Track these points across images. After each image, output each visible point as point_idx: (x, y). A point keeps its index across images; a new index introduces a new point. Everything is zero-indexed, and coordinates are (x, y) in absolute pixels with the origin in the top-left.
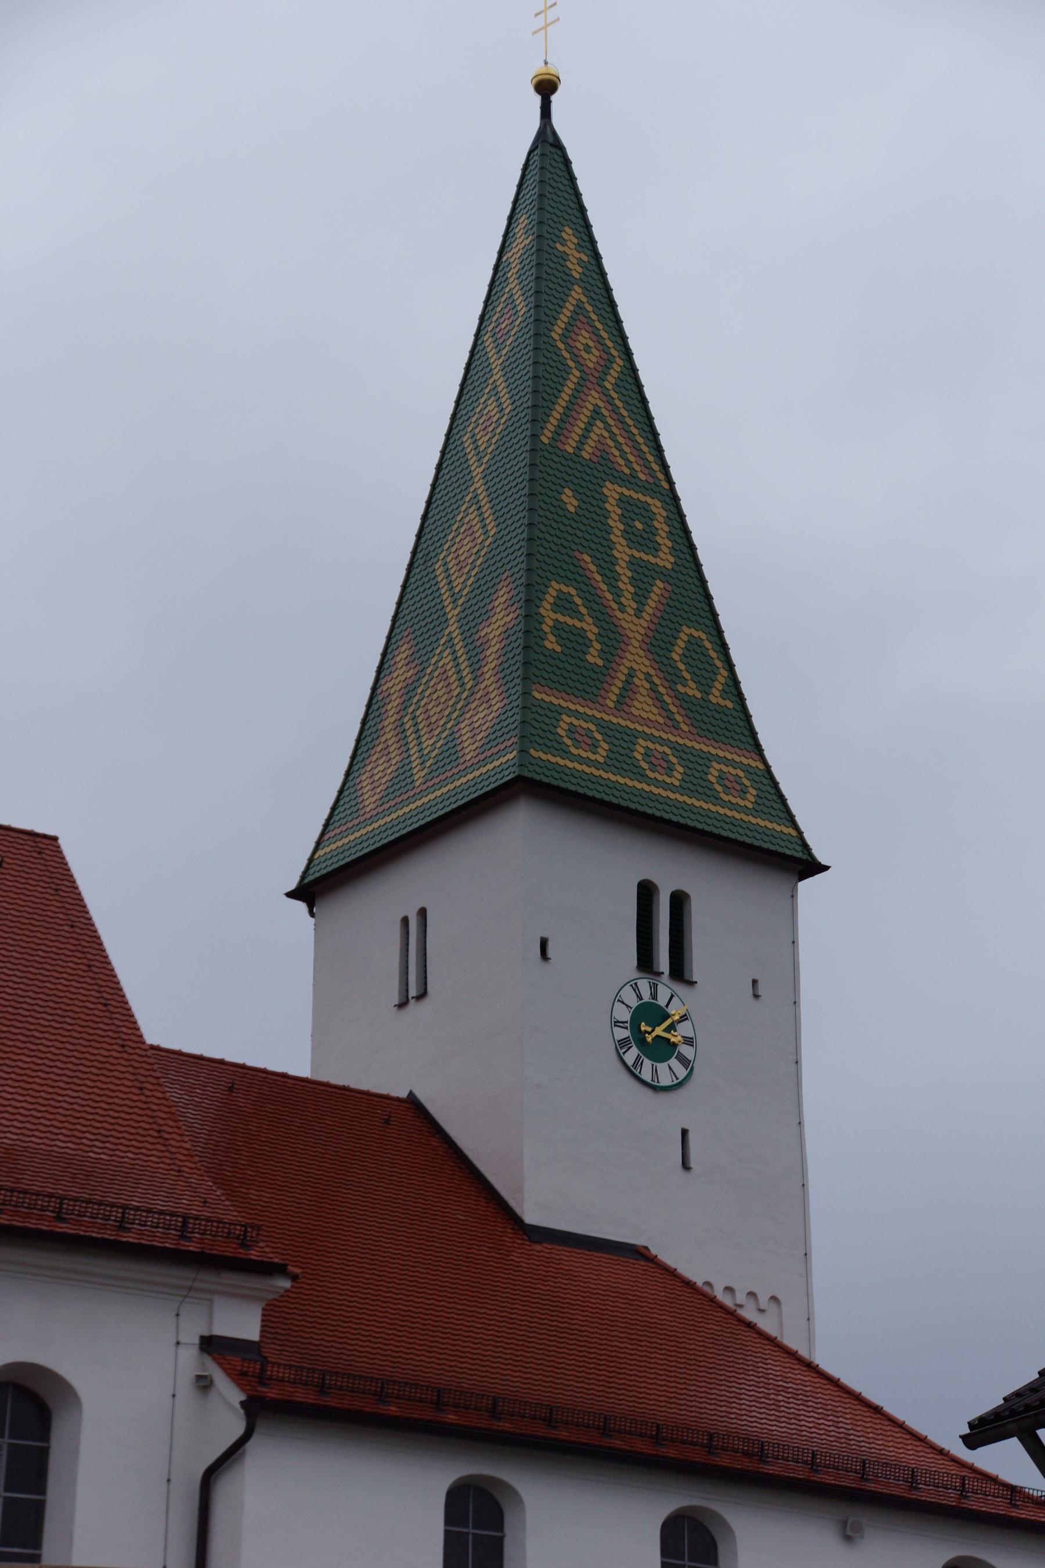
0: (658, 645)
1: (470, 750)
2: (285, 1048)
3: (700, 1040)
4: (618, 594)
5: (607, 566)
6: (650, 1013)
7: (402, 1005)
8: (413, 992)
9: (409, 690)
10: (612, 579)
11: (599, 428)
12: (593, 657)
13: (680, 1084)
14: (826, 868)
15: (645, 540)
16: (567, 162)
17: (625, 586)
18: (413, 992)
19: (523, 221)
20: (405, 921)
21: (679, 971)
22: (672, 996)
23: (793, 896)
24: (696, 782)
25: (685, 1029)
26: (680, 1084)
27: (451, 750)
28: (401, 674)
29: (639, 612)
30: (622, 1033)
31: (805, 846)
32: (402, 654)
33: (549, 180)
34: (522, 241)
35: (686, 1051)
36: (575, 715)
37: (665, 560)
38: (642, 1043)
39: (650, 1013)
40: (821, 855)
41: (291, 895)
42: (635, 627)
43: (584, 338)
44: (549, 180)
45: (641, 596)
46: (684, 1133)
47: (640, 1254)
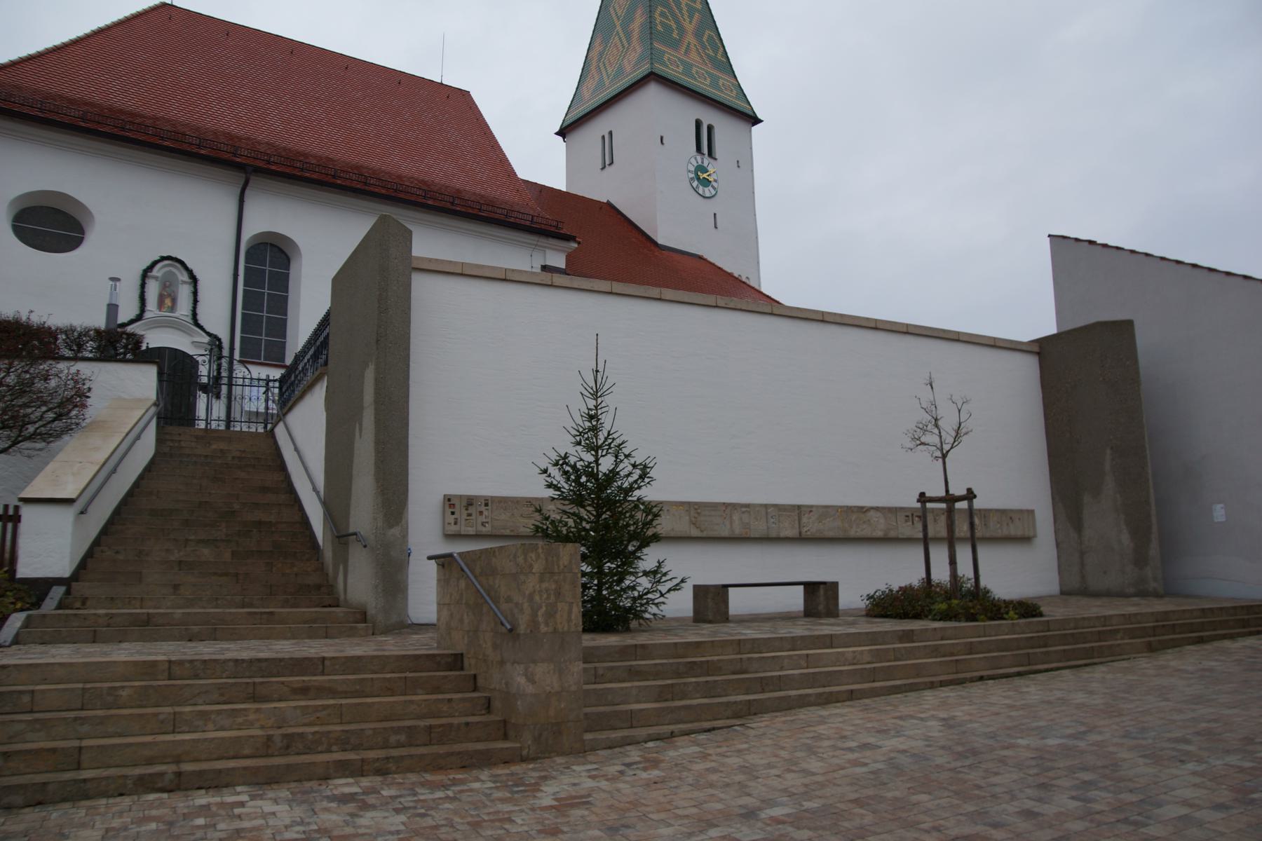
0: (698, 34)
1: (628, 68)
2: (558, 181)
6: (701, 169)
8: (607, 162)
9: (601, 54)
10: (681, 10)
17: (684, 11)
18: (608, 161)
21: (710, 154)
24: (715, 84)
27: (620, 71)
32: (598, 41)
35: (715, 184)
36: (669, 54)
38: (698, 179)
39: (701, 169)
40: (760, 116)
42: (690, 27)
45: (691, 17)
47: (700, 258)
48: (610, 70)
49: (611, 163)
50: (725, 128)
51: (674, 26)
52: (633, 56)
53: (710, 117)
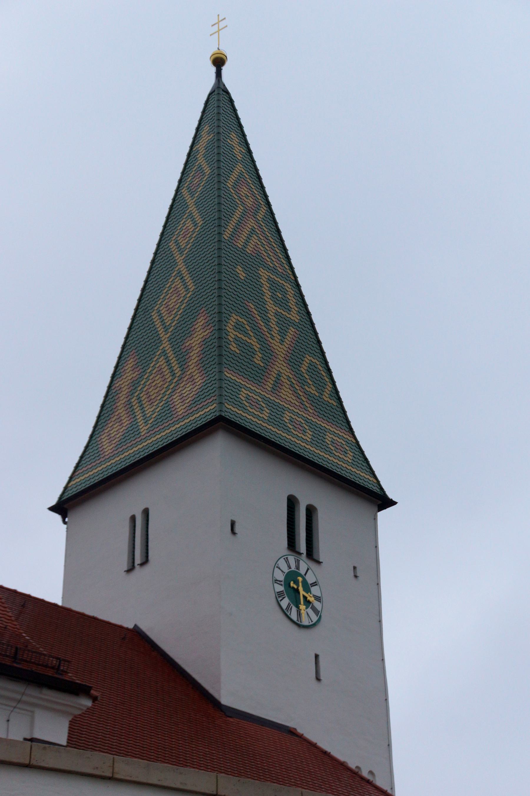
0: (294, 361)
1: (180, 409)
3: (324, 599)
4: (270, 329)
5: (263, 313)
7: (131, 569)
8: (138, 560)
9: (134, 384)
11: (254, 239)
12: (258, 360)
13: (314, 625)
14: (394, 503)
15: (283, 303)
16: (231, 101)
19: (206, 128)
20: (133, 519)
21: (311, 554)
22: (308, 569)
23: (375, 519)
25: (315, 590)
26: (314, 625)
27: (167, 412)
28: (129, 375)
29: (282, 341)
30: (280, 588)
31: (382, 489)
32: (130, 363)
33: (220, 108)
34: (205, 138)
37: (295, 316)
40: (391, 494)
41: (52, 509)
42: (281, 349)
43: (244, 191)
44: (220, 108)
45: (283, 333)
46: (317, 656)
47: (292, 732)
48: (149, 411)
49: (145, 561)
50: (334, 513)
51: (257, 346)
52: (189, 390)
53: (310, 492)
